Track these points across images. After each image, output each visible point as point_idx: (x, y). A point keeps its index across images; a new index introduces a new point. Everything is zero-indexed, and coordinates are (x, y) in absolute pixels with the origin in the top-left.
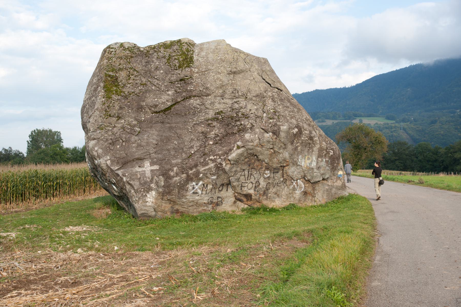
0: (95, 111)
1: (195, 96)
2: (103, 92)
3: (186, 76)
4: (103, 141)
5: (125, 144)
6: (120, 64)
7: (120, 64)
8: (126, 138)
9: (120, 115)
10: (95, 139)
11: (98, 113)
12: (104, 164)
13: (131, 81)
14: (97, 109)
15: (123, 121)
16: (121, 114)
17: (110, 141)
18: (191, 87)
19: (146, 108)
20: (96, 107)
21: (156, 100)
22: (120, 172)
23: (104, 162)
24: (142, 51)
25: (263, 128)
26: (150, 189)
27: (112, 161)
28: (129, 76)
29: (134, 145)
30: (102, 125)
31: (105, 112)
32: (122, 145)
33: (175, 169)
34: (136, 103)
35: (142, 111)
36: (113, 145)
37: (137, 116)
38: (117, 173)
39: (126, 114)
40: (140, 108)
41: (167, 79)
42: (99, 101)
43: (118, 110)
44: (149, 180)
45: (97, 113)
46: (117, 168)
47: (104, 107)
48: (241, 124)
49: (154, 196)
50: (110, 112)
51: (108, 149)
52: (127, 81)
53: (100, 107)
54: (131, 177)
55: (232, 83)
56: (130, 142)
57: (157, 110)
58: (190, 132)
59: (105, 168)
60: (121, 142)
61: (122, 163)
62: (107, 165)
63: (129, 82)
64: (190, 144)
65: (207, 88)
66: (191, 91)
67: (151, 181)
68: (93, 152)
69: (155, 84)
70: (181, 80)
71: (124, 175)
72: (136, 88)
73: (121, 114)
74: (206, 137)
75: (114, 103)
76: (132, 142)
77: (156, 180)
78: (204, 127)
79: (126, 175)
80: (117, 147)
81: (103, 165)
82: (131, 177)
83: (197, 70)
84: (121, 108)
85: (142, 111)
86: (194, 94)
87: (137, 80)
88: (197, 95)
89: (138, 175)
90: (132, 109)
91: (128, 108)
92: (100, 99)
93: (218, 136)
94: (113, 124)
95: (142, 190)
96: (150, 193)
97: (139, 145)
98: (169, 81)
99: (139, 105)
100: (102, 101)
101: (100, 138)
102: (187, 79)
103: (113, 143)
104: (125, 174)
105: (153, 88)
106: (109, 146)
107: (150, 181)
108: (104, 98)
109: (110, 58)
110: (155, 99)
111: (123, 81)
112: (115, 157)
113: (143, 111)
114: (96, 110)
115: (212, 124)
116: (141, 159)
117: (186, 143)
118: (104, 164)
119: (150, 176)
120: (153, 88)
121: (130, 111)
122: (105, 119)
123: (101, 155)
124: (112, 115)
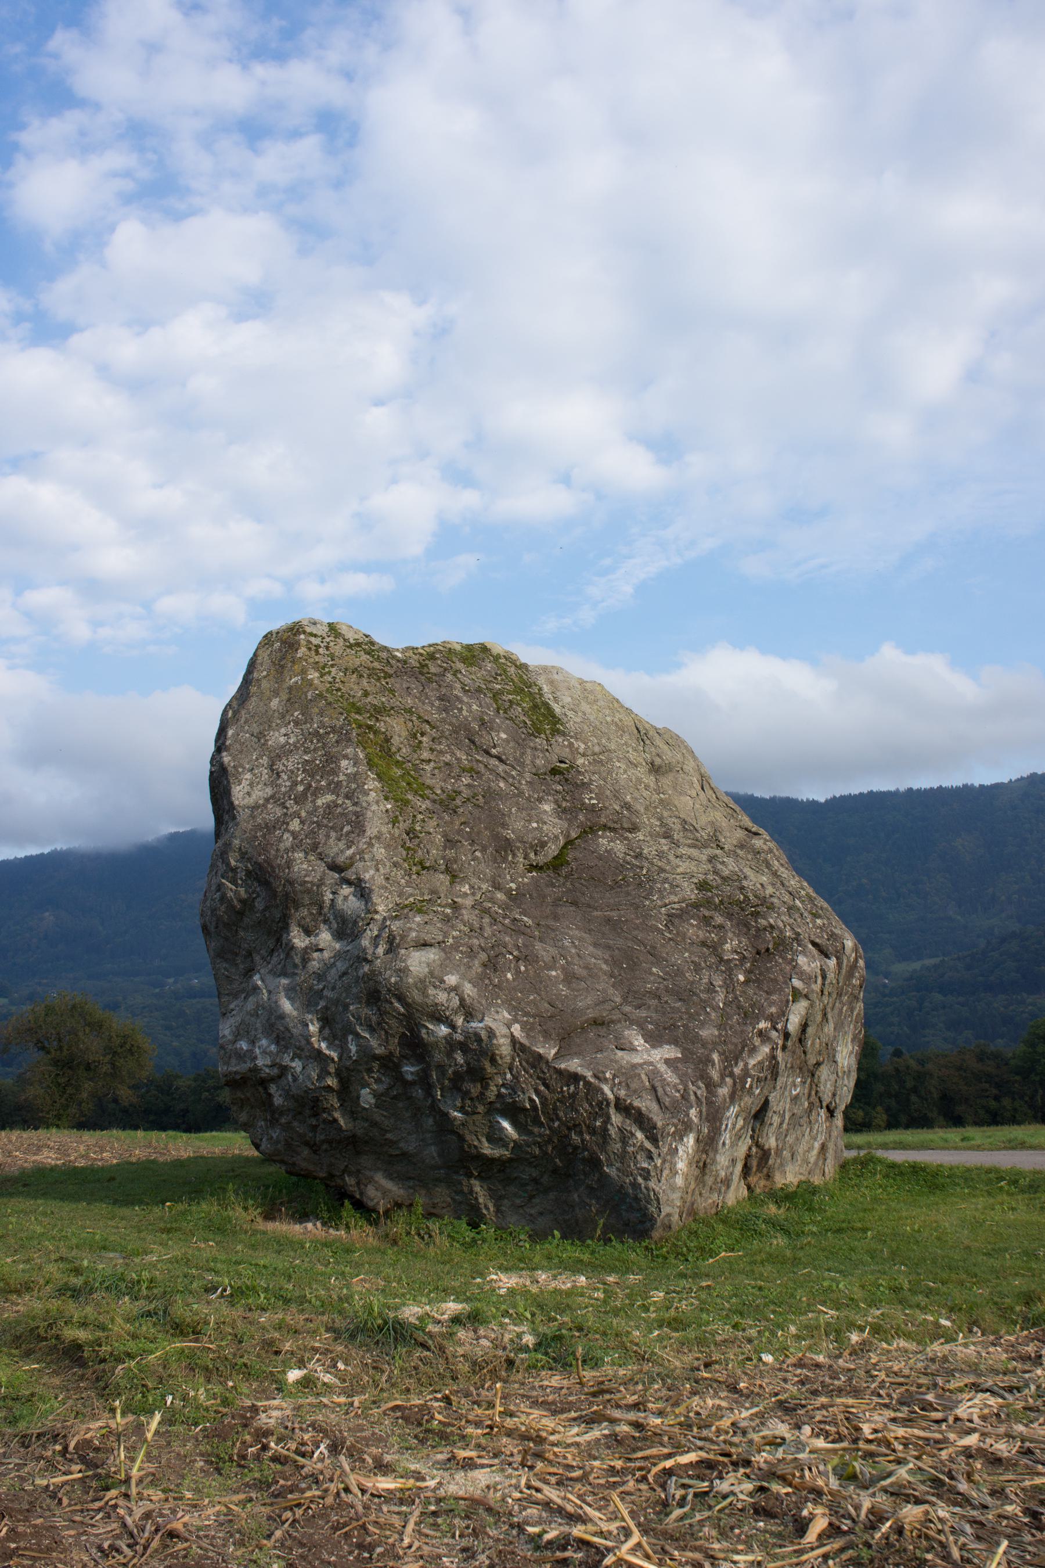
0: (370, 845)
1: (605, 827)
2: (373, 779)
3: (561, 762)
4: (462, 952)
5: (527, 970)
6: (366, 694)
7: (366, 694)
8: (518, 948)
9: (455, 866)
10: (425, 945)
11: (383, 851)
12: (505, 1036)
13: (426, 755)
14: (378, 838)
15: (467, 887)
16: (456, 862)
17: (483, 956)
18: (591, 798)
19: (518, 848)
20: (371, 831)
21: (535, 825)
22: (574, 1065)
23: (504, 1031)
24: (405, 662)
25: (817, 940)
26: (688, 1127)
27: (525, 1027)
28: (414, 736)
29: (554, 973)
30: (411, 895)
31: (404, 853)
32: (518, 972)
33: (715, 1057)
34: (486, 828)
35: (504, 859)
36: (495, 970)
37: (499, 876)
38: (566, 1070)
39: (470, 864)
40: (504, 848)
41: (528, 762)
42: (374, 807)
43: (445, 848)
44: (677, 1095)
45: (379, 851)
46: (553, 1052)
47: (397, 832)
48: (772, 927)
49: (690, 1151)
50: (420, 853)
51: (487, 981)
52: (415, 751)
53: (384, 829)
54: (628, 1085)
55: (661, 800)
56: (537, 962)
57: (541, 859)
58: (670, 939)
59: (505, 1053)
60: (510, 960)
61: (558, 1035)
62: (514, 1040)
63: (422, 757)
64: (701, 979)
65: (627, 806)
66: (592, 809)
67: (684, 1097)
68: (431, 991)
69: (502, 774)
70: (554, 771)
71: (601, 1075)
72: (454, 778)
73: (456, 862)
74: (721, 960)
75: (423, 821)
76: (544, 962)
77: (695, 1094)
78: (699, 927)
79: (608, 1075)
80: (507, 980)
81: (502, 1041)
82: (628, 1085)
83: (583, 746)
84: (450, 843)
85: (504, 859)
86: (603, 820)
87: (441, 752)
88: (611, 824)
89: (643, 1076)
90: (484, 850)
91: (470, 845)
92: (377, 802)
93: (745, 957)
94: (442, 895)
95: (673, 1129)
96: (685, 1140)
97: (570, 978)
98: (534, 771)
99: (496, 837)
100: (387, 811)
101: (444, 942)
102: (567, 769)
103: (492, 965)
104: (604, 1073)
105: (502, 785)
106: (486, 974)
107: (683, 1097)
108: (386, 799)
109: (323, 668)
110: (530, 821)
111: (404, 750)
112: (526, 1014)
113: (510, 858)
114: (373, 841)
115: (712, 918)
116: (603, 1024)
117: (687, 975)
118: (505, 1036)
119: (678, 1081)
120: (502, 785)
121: (478, 854)
122: (414, 877)
123: (476, 1005)
124: (428, 865)
